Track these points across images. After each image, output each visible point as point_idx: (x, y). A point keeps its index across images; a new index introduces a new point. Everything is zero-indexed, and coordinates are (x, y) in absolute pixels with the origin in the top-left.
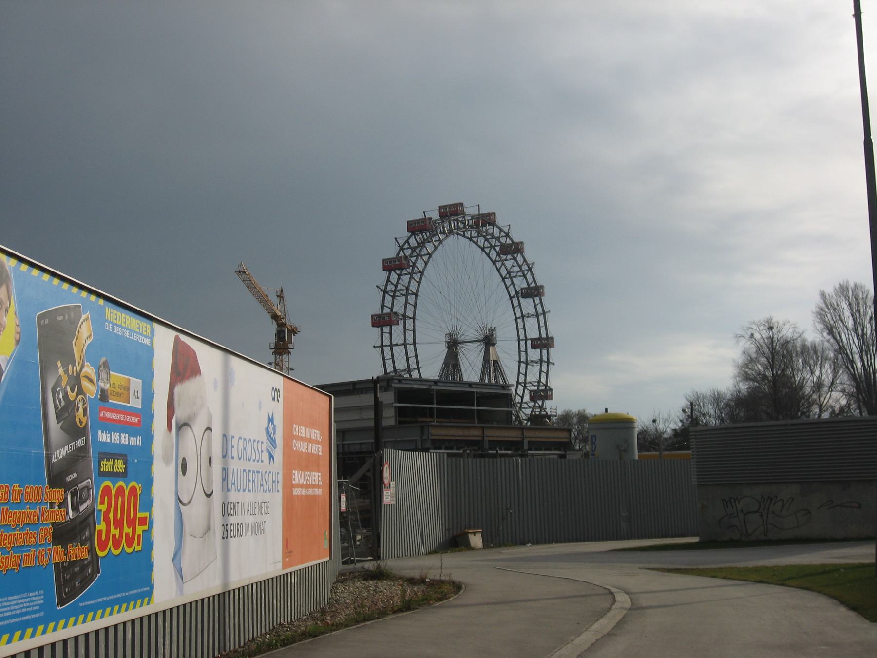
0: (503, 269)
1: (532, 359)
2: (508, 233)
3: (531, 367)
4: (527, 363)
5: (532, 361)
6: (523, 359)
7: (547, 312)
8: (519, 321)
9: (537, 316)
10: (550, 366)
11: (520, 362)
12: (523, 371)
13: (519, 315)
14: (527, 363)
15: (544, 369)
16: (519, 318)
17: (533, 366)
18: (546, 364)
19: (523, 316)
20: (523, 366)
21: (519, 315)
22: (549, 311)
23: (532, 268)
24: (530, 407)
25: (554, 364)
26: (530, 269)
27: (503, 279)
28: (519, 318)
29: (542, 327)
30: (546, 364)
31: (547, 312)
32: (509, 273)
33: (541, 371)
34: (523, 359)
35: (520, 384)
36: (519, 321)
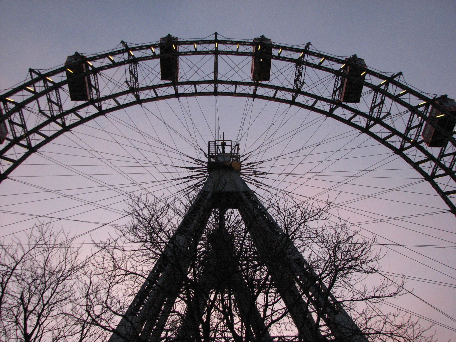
0: (122, 100)
1: (292, 81)
2: (39, 74)
3: (305, 86)
4: (298, 91)
5: (296, 81)
6: (289, 97)
7: (216, 37)
8: (221, 88)
9: (216, 53)
10: (311, 49)
11: (292, 103)
12: (310, 102)
13: (211, 88)
14: (298, 91)
15: (317, 61)
16: (216, 88)
17: (304, 83)
18: (306, 55)
19: (216, 82)
20: (300, 99)
21: (211, 88)
22: (216, 34)
23: (126, 46)
24: (382, 102)
25: (309, 44)
26: (127, 50)
27: (139, 102)
28: (216, 88)
29: (238, 49)
30: (306, 55)
31: (216, 37)
32: (133, 90)
33: (319, 67)
34: (289, 97)
35: (332, 110)
36: (221, 88)
